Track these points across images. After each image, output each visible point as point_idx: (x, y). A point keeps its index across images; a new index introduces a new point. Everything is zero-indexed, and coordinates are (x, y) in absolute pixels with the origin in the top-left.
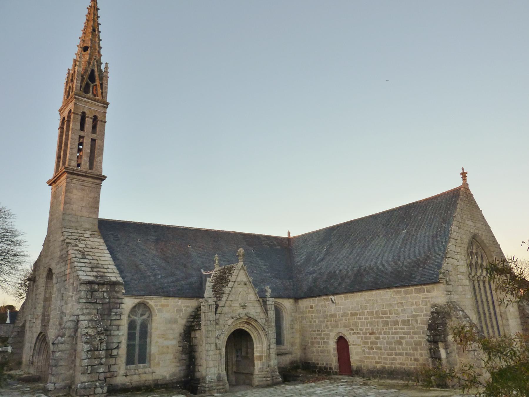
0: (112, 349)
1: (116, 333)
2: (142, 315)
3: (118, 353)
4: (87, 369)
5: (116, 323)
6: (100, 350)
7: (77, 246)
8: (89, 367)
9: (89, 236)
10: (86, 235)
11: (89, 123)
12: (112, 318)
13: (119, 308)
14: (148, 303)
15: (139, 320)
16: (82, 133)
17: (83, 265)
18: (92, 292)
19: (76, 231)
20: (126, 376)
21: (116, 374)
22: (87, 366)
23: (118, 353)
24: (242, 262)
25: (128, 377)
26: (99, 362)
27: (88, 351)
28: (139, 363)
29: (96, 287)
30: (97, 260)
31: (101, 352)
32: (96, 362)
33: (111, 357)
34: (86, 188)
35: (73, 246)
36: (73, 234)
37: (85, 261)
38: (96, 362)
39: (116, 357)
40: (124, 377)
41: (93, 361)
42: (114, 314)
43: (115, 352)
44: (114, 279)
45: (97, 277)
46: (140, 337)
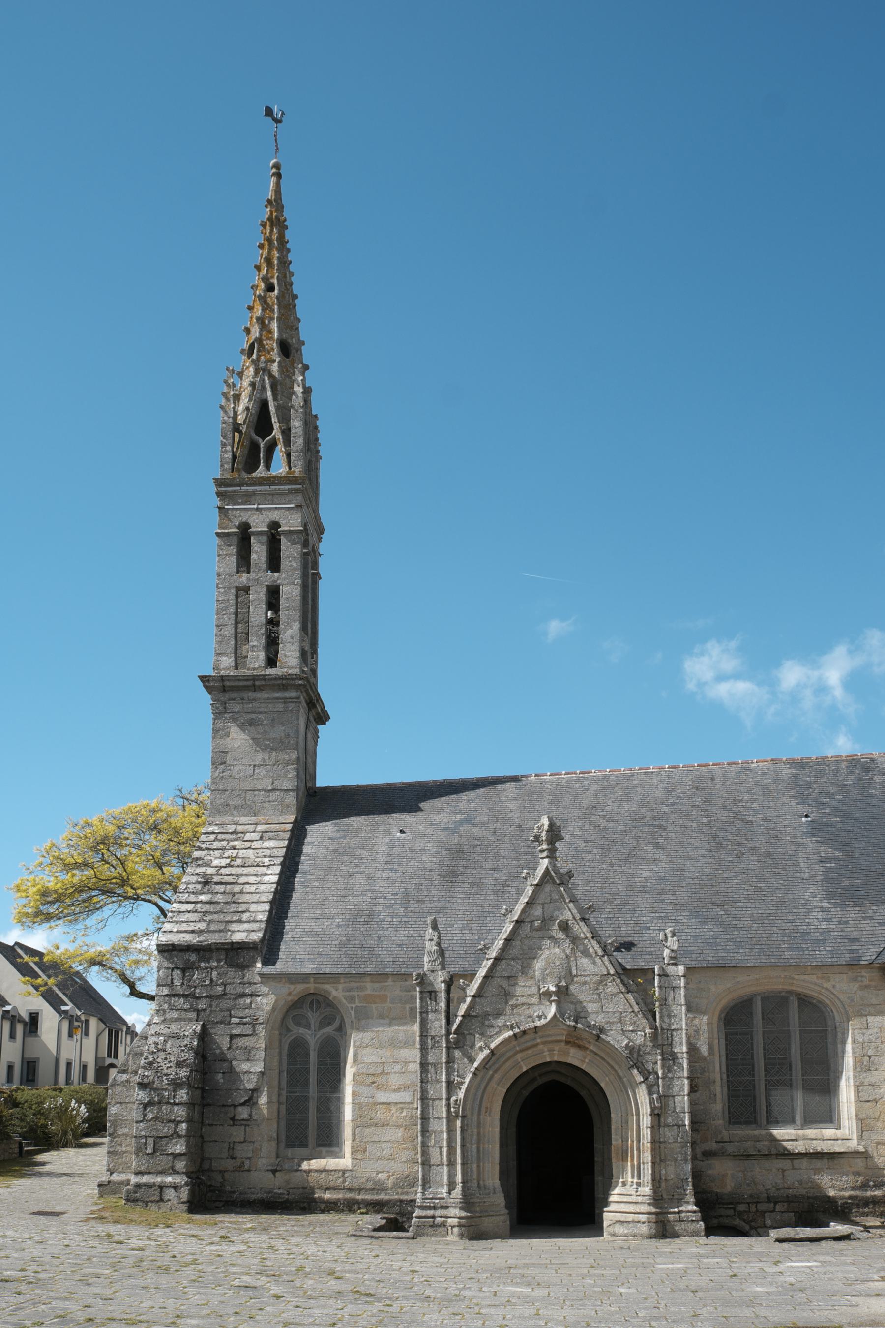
0: (235, 1106)
1: (245, 1066)
2: (323, 1024)
3: (250, 1115)
4: (145, 1144)
5: (242, 1042)
6: (175, 1104)
7: (207, 865)
8: (151, 1141)
9: (255, 836)
10: (248, 836)
11: (259, 552)
12: (234, 1032)
13: (250, 1007)
14: (330, 993)
15: (312, 1038)
16: (244, 579)
17: (190, 907)
18: (184, 971)
19: (231, 828)
20: (274, 1172)
21: (247, 1163)
22: (146, 1137)
23: (250, 1115)
24: (546, 861)
25: (277, 1174)
26: (171, 1132)
27: (145, 1106)
28: (319, 1145)
29: (193, 957)
30: (234, 894)
31: (176, 1108)
32: (167, 1129)
33: (234, 1125)
34: (261, 716)
35: (199, 865)
36: (220, 836)
37: (203, 898)
38: (166, 1130)
39: (246, 1123)
40: (271, 1175)
41: (160, 1126)
42: (238, 1020)
43: (243, 1113)
44: (238, 937)
45: (200, 932)
46: (319, 1082)
